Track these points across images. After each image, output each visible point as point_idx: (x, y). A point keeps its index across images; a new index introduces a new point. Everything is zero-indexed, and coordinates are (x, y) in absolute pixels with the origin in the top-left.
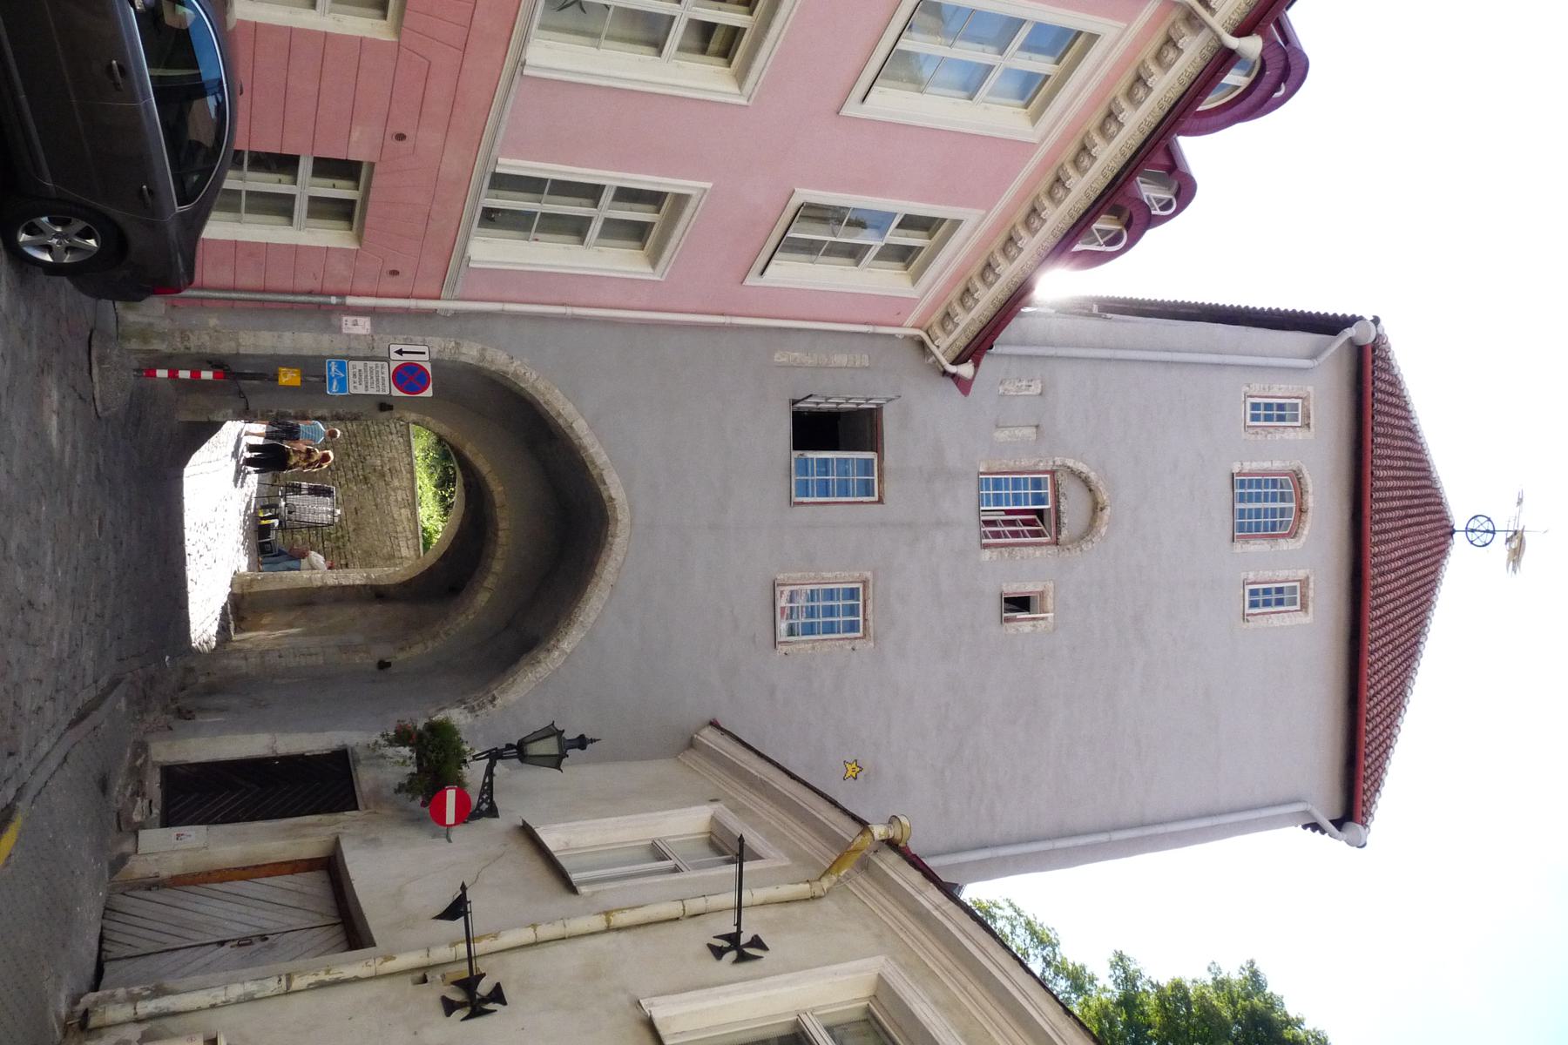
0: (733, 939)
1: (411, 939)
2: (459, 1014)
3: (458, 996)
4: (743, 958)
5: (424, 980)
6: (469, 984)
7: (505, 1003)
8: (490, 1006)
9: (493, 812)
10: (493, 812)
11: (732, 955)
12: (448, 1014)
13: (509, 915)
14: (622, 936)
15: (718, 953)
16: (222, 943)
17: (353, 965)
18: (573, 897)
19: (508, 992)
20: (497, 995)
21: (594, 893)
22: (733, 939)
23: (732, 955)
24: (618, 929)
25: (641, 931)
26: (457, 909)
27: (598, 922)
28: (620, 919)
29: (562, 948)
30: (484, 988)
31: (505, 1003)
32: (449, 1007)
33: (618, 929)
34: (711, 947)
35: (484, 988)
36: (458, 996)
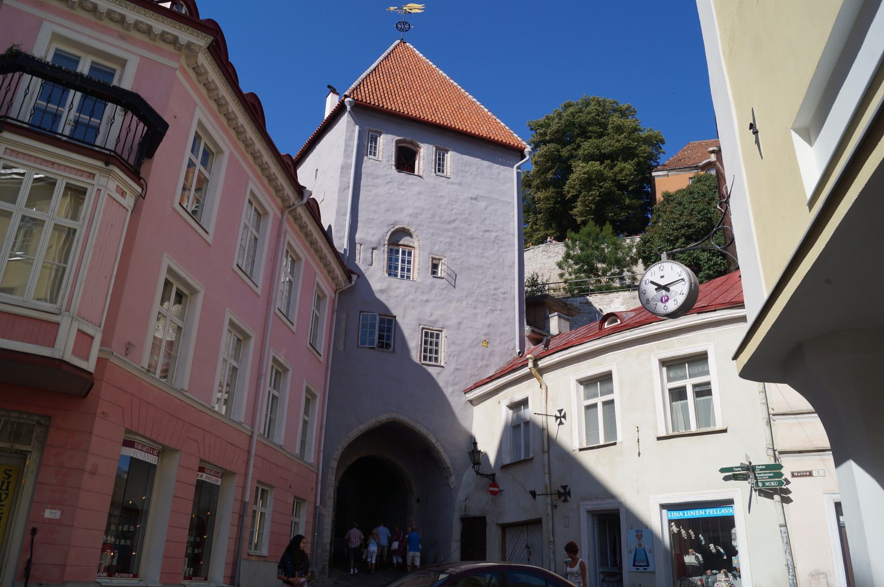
0: (557, 418)
1: (540, 508)
2: (568, 498)
3: (563, 498)
4: (564, 417)
5: (556, 506)
6: (560, 495)
9: (493, 475)
10: (493, 475)
11: (563, 419)
17: (546, 525)
19: (564, 484)
20: (564, 487)
22: (557, 418)
26: (533, 494)
27: (546, 455)
30: (562, 491)
32: (566, 500)
35: (562, 491)
36: (563, 498)
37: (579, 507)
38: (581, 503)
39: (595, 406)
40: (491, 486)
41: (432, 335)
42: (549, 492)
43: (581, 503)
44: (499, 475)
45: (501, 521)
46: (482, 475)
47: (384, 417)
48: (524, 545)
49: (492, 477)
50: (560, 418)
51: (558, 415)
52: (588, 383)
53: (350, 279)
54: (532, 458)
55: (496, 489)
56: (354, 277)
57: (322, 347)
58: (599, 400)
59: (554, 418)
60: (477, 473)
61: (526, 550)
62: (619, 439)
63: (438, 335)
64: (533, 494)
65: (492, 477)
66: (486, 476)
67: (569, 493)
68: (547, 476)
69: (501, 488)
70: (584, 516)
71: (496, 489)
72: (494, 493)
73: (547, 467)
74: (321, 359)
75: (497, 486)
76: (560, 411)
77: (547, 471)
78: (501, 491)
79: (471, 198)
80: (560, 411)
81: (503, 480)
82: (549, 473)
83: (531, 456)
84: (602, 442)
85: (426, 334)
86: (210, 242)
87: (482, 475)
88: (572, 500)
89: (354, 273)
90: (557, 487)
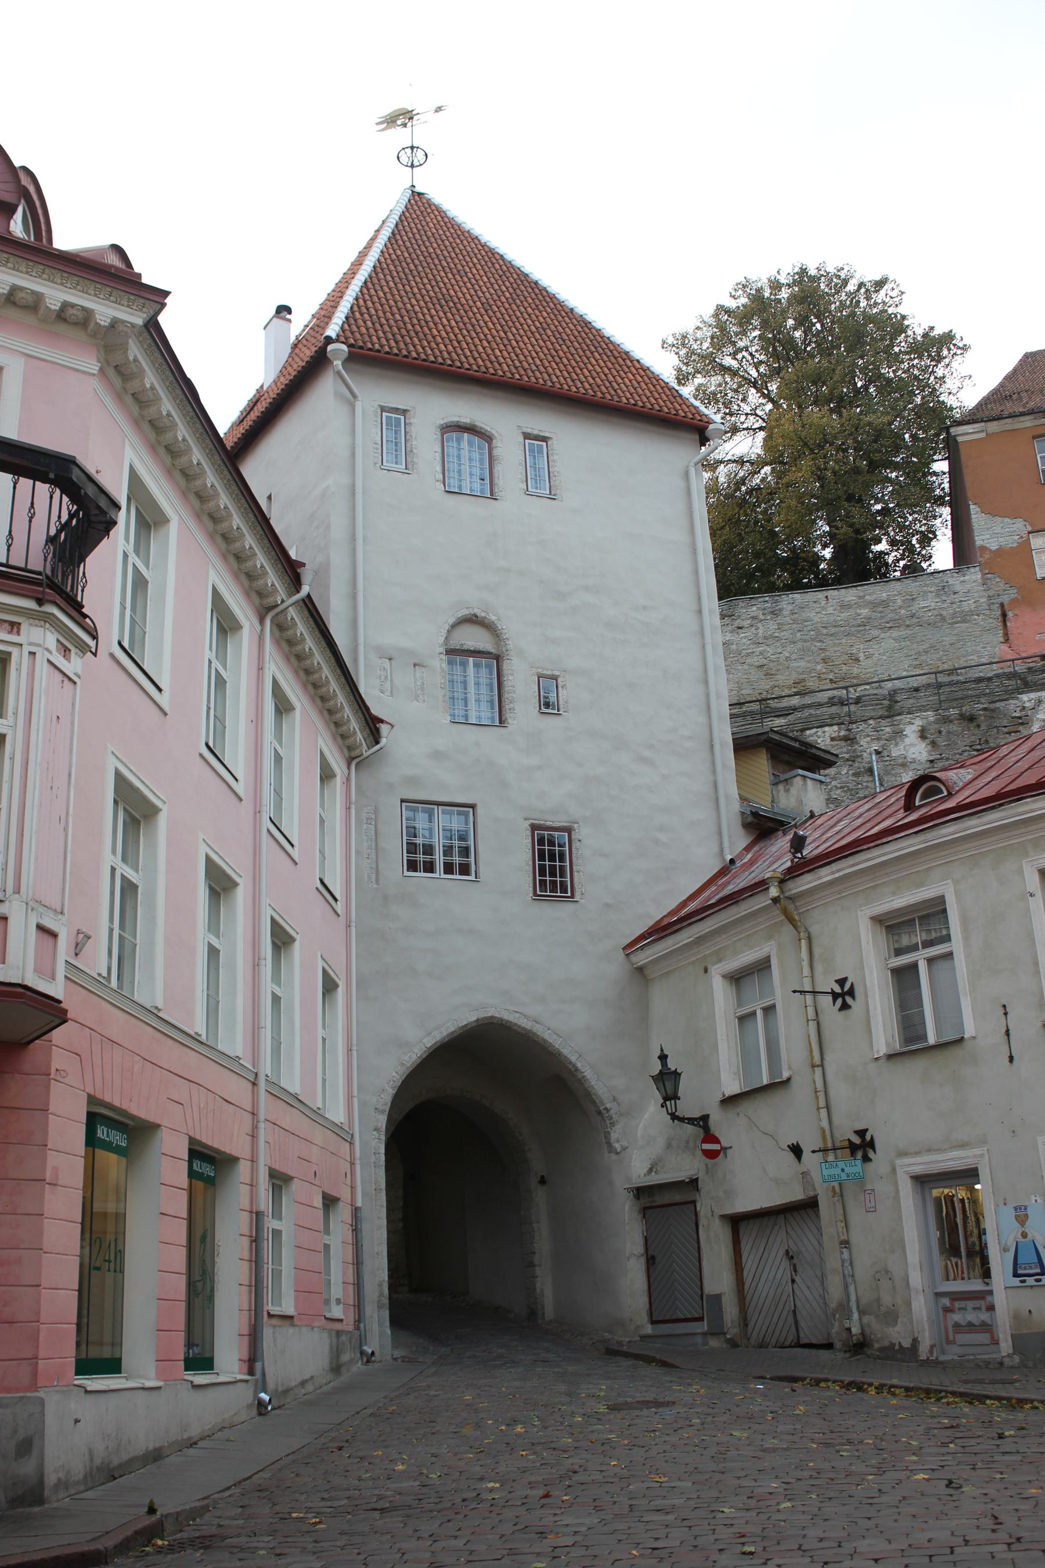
0: (835, 996)
4: (851, 993)
6: (853, 1148)
7: (867, 1130)
8: (868, 1137)
11: (848, 999)
12: (870, 1160)
13: (796, 1119)
14: (828, 1057)
15: (845, 1006)
16: (793, 1281)
18: (792, 1080)
19: (860, 1127)
20: (861, 1133)
21: (790, 1068)
22: (835, 996)
23: (848, 999)
24: (822, 1059)
25: (824, 1046)
26: (796, 1151)
27: (818, 1071)
28: (817, 1059)
29: (832, 1093)
30: (857, 1140)
31: (867, 1130)
32: (866, 1159)
33: (822, 1059)
34: (840, 1009)
35: (857, 1140)
37: (894, 1170)
38: (899, 1162)
39: (914, 967)
40: (704, 1141)
42: (830, 1145)
43: (899, 1162)
44: (716, 1117)
45: (729, 1211)
46: (682, 1120)
47: (468, 1017)
48: (782, 1252)
49: (703, 1121)
50: (842, 995)
51: (837, 989)
52: (892, 925)
54: (789, 1079)
55: (716, 1147)
58: (920, 957)
59: (830, 998)
60: (674, 1117)
61: (786, 1264)
64: (796, 1151)
65: (703, 1121)
66: (691, 1121)
67: (871, 1144)
68: (823, 1113)
69: (724, 1144)
70: (906, 1189)
71: (716, 1147)
72: (711, 1155)
73: (821, 1095)
75: (716, 1141)
77: (822, 1103)
78: (724, 1149)
80: (841, 982)
81: (729, 1129)
82: (828, 1107)
83: (785, 1075)
84: (932, 1040)
87: (682, 1120)
88: (880, 1158)
90: (846, 1132)
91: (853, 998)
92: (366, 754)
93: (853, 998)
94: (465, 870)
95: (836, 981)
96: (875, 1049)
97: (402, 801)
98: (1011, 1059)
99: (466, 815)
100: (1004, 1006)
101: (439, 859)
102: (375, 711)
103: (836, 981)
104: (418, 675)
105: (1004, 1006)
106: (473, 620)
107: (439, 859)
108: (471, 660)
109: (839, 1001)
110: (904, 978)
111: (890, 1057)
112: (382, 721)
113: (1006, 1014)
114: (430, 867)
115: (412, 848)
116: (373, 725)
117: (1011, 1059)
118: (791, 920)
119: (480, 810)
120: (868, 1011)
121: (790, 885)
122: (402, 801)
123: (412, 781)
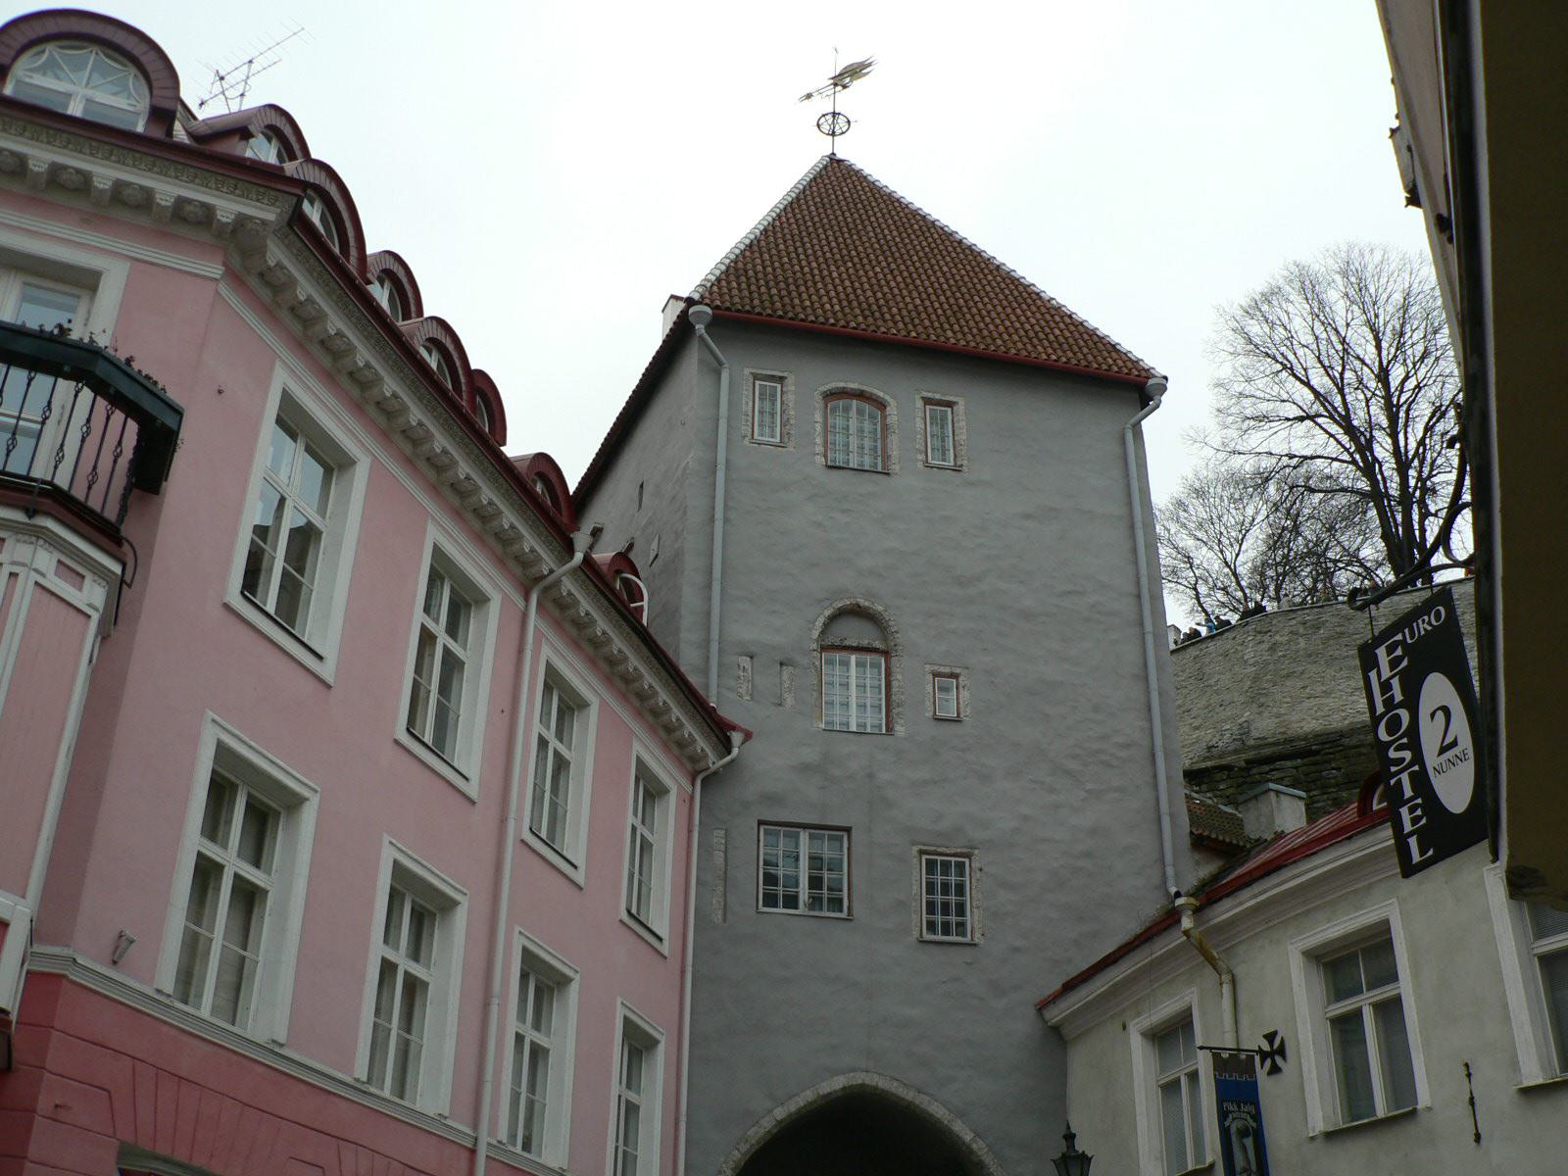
0: (1264, 1055)
4: (1281, 1051)
11: (1278, 1060)
23: (1278, 1060)
34: (1270, 1073)
39: (1356, 1015)
41: (946, 865)
50: (1271, 1055)
51: (1266, 1047)
53: (727, 747)
56: (736, 738)
57: (661, 919)
58: (1365, 1002)
62: (1424, 1099)
63: (960, 866)
74: (665, 949)
76: (1270, 1037)
79: (1028, 517)
84: (1381, 1111)
85: (931, 865)
86: (330, 680)
89: (734, 728)
91: (1284, 1058)
92: (713, 768)
93: (1284, 1058)
94: (836, 903)
95: (1265, 1036)
96: (1310, 1125)
97: (760, 823)
98: (1478, 1138)
99: (840, 839)
100: (1467, 1065)
101: (804, 892)
102: (727, 712)
103: (1265, 1036)
104: (785, 676)
105: (1467, 1065)
106: (856, 612)
107: (804, 892)
108: (853, 658)
109: (1268, 1062)
110: (1346, 1028)
111: (1330, 1136)
112: (734, 728)
113: (1469, 1075)
114: (792, 901)
115: (771, 879)
116: (720, 731)
117: (1478, 1138)
118: (1212, 961)
119: (854, 832)
120: (1301, 1076)
121: (1210, 913)
122: (760, 823)
123: (772, 799)
